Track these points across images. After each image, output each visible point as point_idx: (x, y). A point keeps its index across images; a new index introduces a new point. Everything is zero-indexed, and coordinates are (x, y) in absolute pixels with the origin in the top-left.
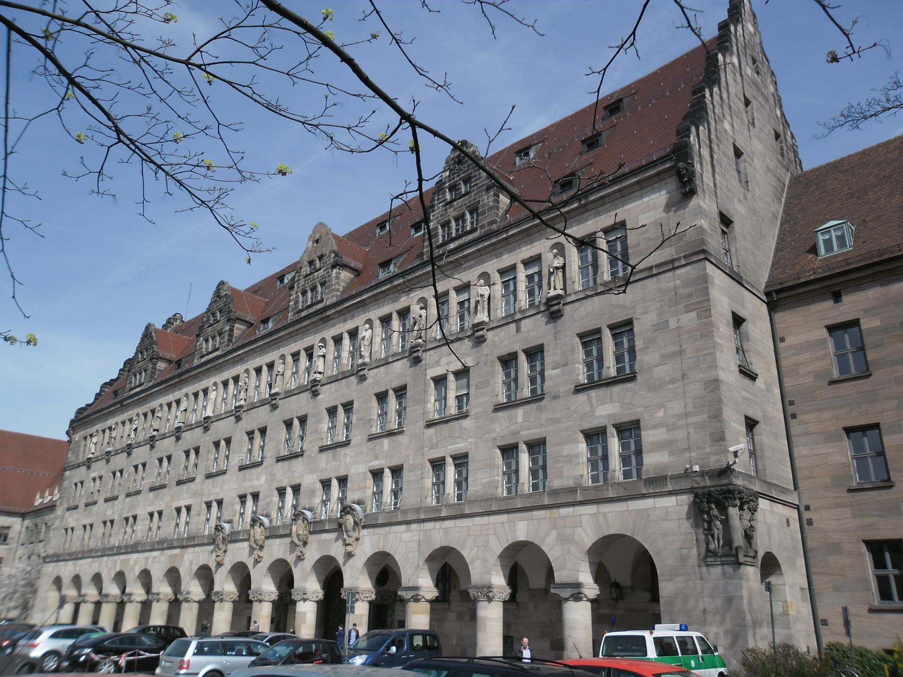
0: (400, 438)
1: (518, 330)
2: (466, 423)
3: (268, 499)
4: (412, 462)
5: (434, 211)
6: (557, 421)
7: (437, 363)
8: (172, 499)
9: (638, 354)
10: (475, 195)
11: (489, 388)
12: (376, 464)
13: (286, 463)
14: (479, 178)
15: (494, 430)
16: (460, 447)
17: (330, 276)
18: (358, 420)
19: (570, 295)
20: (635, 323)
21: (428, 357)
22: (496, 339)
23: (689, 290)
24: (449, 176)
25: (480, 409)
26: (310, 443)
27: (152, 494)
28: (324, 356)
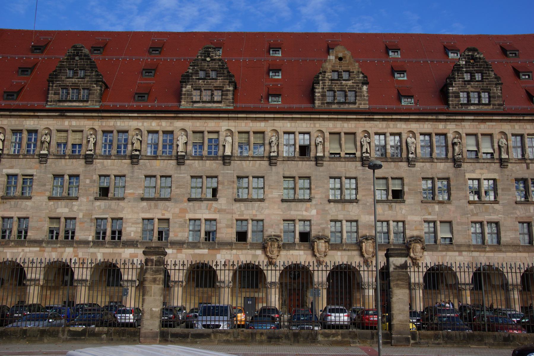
0: (448, 206)
1: (528, 168)
2: (496, 206)
3: (323, 226)
4: (459, 220)
5: (455, 81)
7: (473, 171)
8: (184, 211)
10: (487, 84)
12: (430, 218)
13: (340, 206)
14: (489, 76)
15: (516, 214)
16: (494, 217)
18: (409, 189)
21: (465, 166)
22: (514, 169)
24: (465, 65)
25: (506, 202)
26: (364, 196)
27: (144, 204)
28: (369, 143)
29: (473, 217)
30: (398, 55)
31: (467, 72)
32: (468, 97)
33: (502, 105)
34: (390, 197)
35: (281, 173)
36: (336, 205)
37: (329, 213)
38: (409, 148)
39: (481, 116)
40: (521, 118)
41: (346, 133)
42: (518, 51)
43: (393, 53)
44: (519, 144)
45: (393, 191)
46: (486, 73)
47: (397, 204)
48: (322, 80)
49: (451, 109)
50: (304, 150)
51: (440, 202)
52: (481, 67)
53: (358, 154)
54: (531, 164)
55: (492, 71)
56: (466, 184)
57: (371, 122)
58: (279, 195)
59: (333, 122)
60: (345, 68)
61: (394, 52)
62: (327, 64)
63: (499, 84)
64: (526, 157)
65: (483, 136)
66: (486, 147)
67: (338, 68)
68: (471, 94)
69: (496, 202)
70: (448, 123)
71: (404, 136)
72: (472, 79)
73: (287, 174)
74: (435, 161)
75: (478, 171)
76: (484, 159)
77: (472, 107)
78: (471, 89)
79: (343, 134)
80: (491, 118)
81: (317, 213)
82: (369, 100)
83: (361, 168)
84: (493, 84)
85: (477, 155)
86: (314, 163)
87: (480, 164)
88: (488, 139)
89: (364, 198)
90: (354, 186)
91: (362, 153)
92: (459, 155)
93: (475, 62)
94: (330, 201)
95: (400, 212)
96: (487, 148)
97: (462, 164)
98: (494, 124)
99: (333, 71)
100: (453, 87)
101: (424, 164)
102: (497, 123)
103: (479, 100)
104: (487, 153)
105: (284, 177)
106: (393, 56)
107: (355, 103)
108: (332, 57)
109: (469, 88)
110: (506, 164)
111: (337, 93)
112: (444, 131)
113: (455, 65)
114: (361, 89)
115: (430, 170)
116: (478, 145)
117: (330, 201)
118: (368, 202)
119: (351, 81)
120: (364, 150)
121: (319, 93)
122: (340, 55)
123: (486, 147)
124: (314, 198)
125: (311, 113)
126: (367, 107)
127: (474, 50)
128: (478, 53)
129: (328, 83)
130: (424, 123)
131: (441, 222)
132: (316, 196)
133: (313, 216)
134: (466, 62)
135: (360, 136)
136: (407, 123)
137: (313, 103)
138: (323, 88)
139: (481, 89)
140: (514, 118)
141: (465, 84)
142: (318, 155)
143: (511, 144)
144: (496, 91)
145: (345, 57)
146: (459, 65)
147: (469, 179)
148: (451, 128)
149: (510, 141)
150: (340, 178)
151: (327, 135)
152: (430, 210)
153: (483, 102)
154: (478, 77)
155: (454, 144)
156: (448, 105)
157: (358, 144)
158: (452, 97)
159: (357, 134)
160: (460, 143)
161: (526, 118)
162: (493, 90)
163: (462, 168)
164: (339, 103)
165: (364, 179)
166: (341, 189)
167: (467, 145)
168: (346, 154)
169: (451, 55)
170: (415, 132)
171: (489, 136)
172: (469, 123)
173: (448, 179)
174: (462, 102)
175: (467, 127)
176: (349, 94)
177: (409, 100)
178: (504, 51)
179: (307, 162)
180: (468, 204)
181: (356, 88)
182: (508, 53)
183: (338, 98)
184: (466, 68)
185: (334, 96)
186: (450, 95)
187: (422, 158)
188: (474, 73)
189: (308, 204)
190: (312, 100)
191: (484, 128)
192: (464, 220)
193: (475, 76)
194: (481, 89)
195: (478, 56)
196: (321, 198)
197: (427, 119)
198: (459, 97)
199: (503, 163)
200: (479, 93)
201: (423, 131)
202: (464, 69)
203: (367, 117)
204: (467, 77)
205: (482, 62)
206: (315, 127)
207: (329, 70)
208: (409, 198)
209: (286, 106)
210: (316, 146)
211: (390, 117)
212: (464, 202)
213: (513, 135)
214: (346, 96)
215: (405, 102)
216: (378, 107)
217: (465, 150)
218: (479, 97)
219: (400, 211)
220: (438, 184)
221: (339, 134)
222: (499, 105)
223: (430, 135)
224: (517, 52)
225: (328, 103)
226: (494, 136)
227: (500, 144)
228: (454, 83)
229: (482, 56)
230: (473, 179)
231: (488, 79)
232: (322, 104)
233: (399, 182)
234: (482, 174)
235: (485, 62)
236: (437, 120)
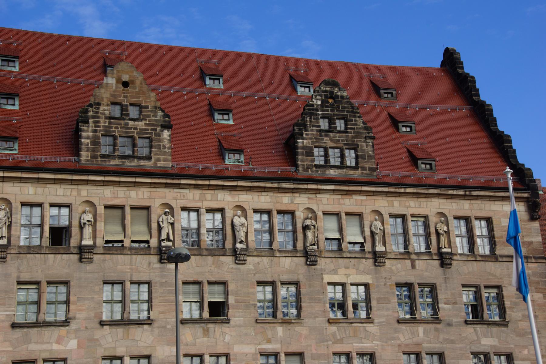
0: (298, 328)
1: (413, 267)
4: (314, 351)
5: (306, 130)
6: (453, 342)
9: (507, 310)
10: (353, 137)
11: (390, 305)
12: (269, 347)
13: (120, 331)
14: (356, 125)
15: (399, 339)
16: (367, 346)
17: (159, 135)
18: (237, 301)
19: (456, 255)
20: (504, 289)
21: (322, 263)
22: (394, 268)
23: (537, 279)
24: (322, 106)
25: (383, 320)
28: (172, 224)
29: (336, 345)
30: (219, 85)
31: (323, 117)
32: (326, 155)
33: (374, 169)
34: (206, 315)
35: (14, 276)
36: (114, 330)
37: (100, 345)
38: (237, 233)
39: (345, 185)
40: (402, 190)
41: (133, 208)
42: (395, 90)
43: (212, 81)
44: (400, 230)
45: (210, 303)
46: (352, 120)
47: (217, 326)
48: (93, 117)
49: (301, 173)
50: (59, 236)
51: (285, 322)
52: (343, 111)
53: (154, 242)
54: (417, 261)
55: (360, 117)
56: (324, 292)
57: (176, 190)
58: (7, 315)
59: (111, 188)
60: (133, 100)
61: (214, 79)
62: (103, 91)
63: (370, 138)
64: (410, 249)
65: (348, 217)
66: (353, 234)
67: (120, 99)
68: (331, 152)
69: (369, 320)
70: (297, 195)
71: (229, 214)
72: (332, 128)
73: (25, 277)
74: (278, 254)
75: (342, 271)
76: (350, 252)
77: (332, 172)
78: (329, 144)
79: (128, 210)
80: (359, 188)
81: (79, 346)
82: (172, 154)
83: (158, 265)
84: (361, 137)
85: (340, 245)
86: (76, 257)
87: (344, 259)
88: (356, 219)
89: (162, 316)
90: (145, 296)
91: (160, 241)
92: (314, 245)
93: (335, 101)
94: (102, 323)
95: (222, 339)
96: (355, 235)
97: (319, 259)
98: (364, 198)
99: (113, 103)
100: (303, 139)
101: (259, 259)
102: (369, 197)
103: (342, 162)
104: (355, 243)
105: (19, 283)
106: (212, 86)
107: (149, 158)
108: (110, 80)
109: (327, 141)
110: (382, 260)
111: (120, 140)
112: (291, 208)
113: (307, 105)
114: (160, 136)
115: (269, 270)
116: (340, 230)
117: (102, 323)
118: (168, 323)
119: (143, 122)
120: (164, 236)
121: (88, 138)
122: (126, 78)
123: (353, 234)
124: (74, 318)
125: (73, 171)
126: (170, 164)
127: (334, 84)
128: (339, 89)
129: (103, 122)
130: (259, 194)
131: (287, 354)
132: (78, 316)
133: (71, 350)
134: (322, 101)
135: (156, 212)
136: (233, 192)
137: (78, 155)
138: (95, 131)
139: (345, 144)
140: (392, 190)
141: (321, 135)
142: (84, 243)
143: (389, 229)
144: (366, 148)
145: (133, 82)
146: (313, 105)
147: (329, 284)
148: (300, 203)
149: (387, 224)
150: (122, 283)
151: (101, 210)
152: (269, 334)
153: (348, 164)
154: (340, 125)
155: (305, 228)
156: (296, 166)
157: (154, 225)
158: (303, 155)
159: (153, 209)
160: (314, 226)
161: (408, 190)
162: (362, 146)
163: (318, 267)
164: (122, 157)
165: (162, 284)
166: (123, 302)
167: (326, 230)
168: (133, 242)
169: (301, 90)
170: (246, 207)
171: (357, 217)
172: (328, 196)
173: (296, 284)
174: (317, 163)
175: (325, 201)
176: (139, 142)
177: (237, 156)
178: (376, 89)
179: (64, 256)
180: (327, 324)
181: (151, 133)
182: (382, 92)
183: (120, 149)
184: (322, 111)
185: (115, 145)
186: (300, 151)
187: (256, 250)
188: (334, 119)
189: (63, 330)
190: (75, 148)
191: (349, 204)
192: (322, 350)
193: (335, 123)
194: (345, 144)
195: (339, 93)
196: (87, 319)
197: (265, 187)
198: (311, 154)
199: (377, 258)
200: (342, 150)
201: (259, 206)
202: (320, 113)
203: (169, 181)
204: (324, 124)
205: (345, 103)
206: (79, 195)
207: (105, 101)
208: (236, 316)
209: (27, 158)
210: (81, 228)
211: (207, 183)
212: (321, 321)
213: (391, 216)
214: (134, 146)
215: (230, 160)
216: (187, 166)
217: (322, 237)
218: (342, 156)
219: (221, 337)
220: (283, 292)
221: (121, 208)
222: (371, 169)
223: (268, 212)
224: (394, 92)
225: (103, 156)
226: (365, 216)
227: (373, 229)
228: (304, 133)
229: (345, 94)
230: (334, 284)
231: (354, 129)
232: (93, 156)
233: (219, 289)
234: (347, 276)
235: (350, 104)
236: (280, 190)
